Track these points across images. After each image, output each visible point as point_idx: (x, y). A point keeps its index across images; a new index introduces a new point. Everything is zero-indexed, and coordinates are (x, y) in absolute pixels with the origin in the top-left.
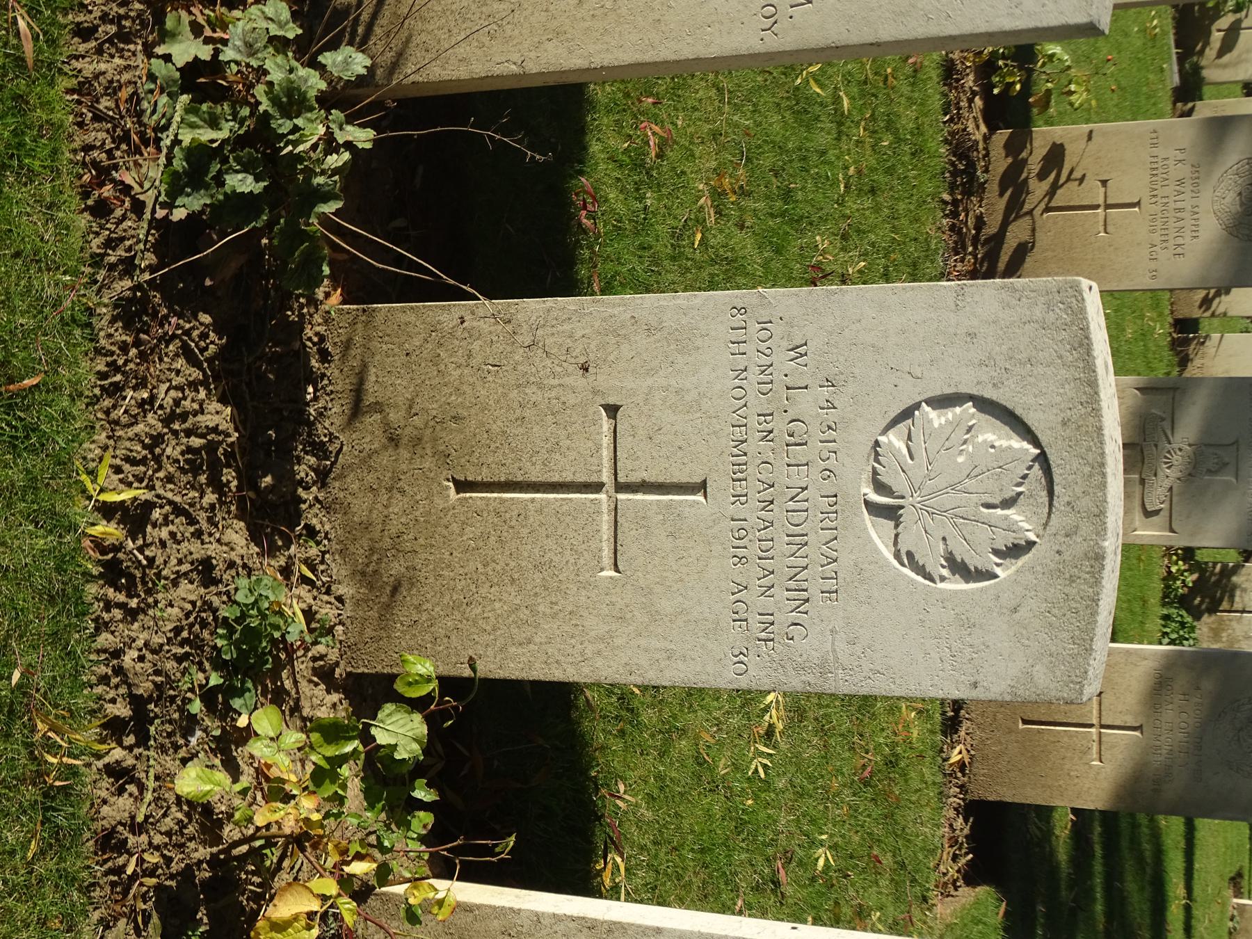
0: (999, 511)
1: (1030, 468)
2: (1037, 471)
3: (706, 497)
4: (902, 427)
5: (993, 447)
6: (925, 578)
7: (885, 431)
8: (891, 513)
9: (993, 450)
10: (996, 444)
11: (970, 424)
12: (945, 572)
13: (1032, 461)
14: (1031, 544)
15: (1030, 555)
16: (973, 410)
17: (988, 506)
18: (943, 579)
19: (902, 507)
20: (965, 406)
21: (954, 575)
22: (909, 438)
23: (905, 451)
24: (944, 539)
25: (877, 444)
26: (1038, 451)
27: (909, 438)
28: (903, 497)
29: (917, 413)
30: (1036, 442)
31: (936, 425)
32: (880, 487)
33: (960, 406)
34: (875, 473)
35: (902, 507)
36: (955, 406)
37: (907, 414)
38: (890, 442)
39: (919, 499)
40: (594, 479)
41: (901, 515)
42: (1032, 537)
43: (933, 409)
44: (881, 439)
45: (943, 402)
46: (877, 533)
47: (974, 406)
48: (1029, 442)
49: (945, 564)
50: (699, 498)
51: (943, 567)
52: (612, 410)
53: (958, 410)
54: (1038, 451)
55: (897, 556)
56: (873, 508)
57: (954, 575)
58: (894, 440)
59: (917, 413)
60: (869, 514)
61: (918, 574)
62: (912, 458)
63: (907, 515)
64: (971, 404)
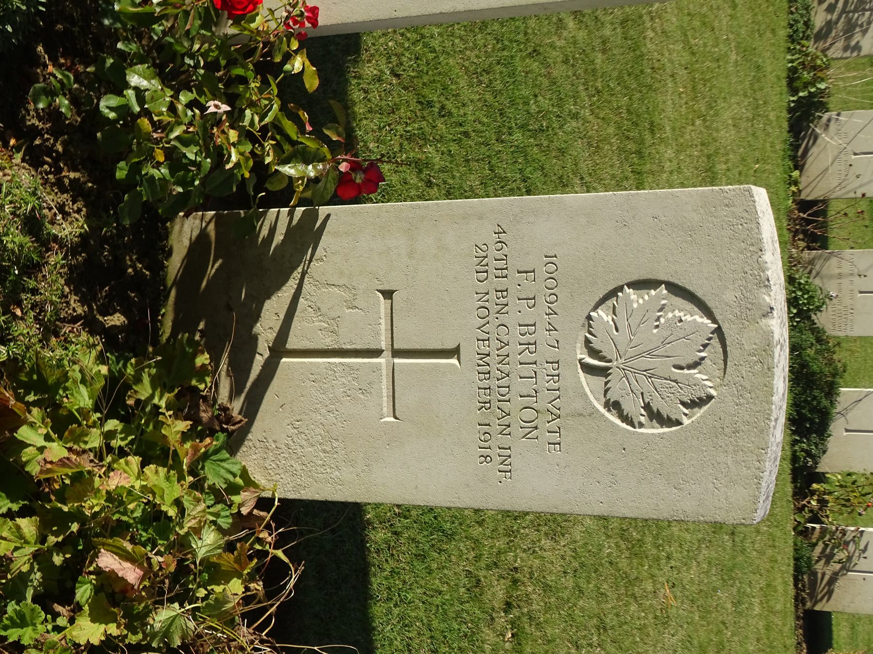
0: (686, 371)
5: (681, 321)
6: (627, 424)
7: (595, 308)
8: (603, 372)
10: (683, 319)
11: (664, 302)
13: (712, 333)
14: (710, 398)
15: (709, 404)
16: (665, 292)
18: (641, 425)
21: (651, 421)
22: (614, 313)
23: (612, 323)
25: (589, 318)
26: (716, 326)
27: (614, 313)
28: (610, 361)
29: (620, 294)
31: (635, 306)
32: (594, 353)
33: (655, 290)
34: (587, 342)
35: (609, 368)
36: (650, 289)
37: (613, 293)
40: (373, 346)
41: (610, 374)
47: (666, 289)
48: (708, 319)
52: (388, 294)
53: (653, 292)
54: (716, 326)
55: (607, 405)
56: (588, 369)
58: (603, 315)
59: (620, 294)
62: (617, 330)
63: (615, 374)
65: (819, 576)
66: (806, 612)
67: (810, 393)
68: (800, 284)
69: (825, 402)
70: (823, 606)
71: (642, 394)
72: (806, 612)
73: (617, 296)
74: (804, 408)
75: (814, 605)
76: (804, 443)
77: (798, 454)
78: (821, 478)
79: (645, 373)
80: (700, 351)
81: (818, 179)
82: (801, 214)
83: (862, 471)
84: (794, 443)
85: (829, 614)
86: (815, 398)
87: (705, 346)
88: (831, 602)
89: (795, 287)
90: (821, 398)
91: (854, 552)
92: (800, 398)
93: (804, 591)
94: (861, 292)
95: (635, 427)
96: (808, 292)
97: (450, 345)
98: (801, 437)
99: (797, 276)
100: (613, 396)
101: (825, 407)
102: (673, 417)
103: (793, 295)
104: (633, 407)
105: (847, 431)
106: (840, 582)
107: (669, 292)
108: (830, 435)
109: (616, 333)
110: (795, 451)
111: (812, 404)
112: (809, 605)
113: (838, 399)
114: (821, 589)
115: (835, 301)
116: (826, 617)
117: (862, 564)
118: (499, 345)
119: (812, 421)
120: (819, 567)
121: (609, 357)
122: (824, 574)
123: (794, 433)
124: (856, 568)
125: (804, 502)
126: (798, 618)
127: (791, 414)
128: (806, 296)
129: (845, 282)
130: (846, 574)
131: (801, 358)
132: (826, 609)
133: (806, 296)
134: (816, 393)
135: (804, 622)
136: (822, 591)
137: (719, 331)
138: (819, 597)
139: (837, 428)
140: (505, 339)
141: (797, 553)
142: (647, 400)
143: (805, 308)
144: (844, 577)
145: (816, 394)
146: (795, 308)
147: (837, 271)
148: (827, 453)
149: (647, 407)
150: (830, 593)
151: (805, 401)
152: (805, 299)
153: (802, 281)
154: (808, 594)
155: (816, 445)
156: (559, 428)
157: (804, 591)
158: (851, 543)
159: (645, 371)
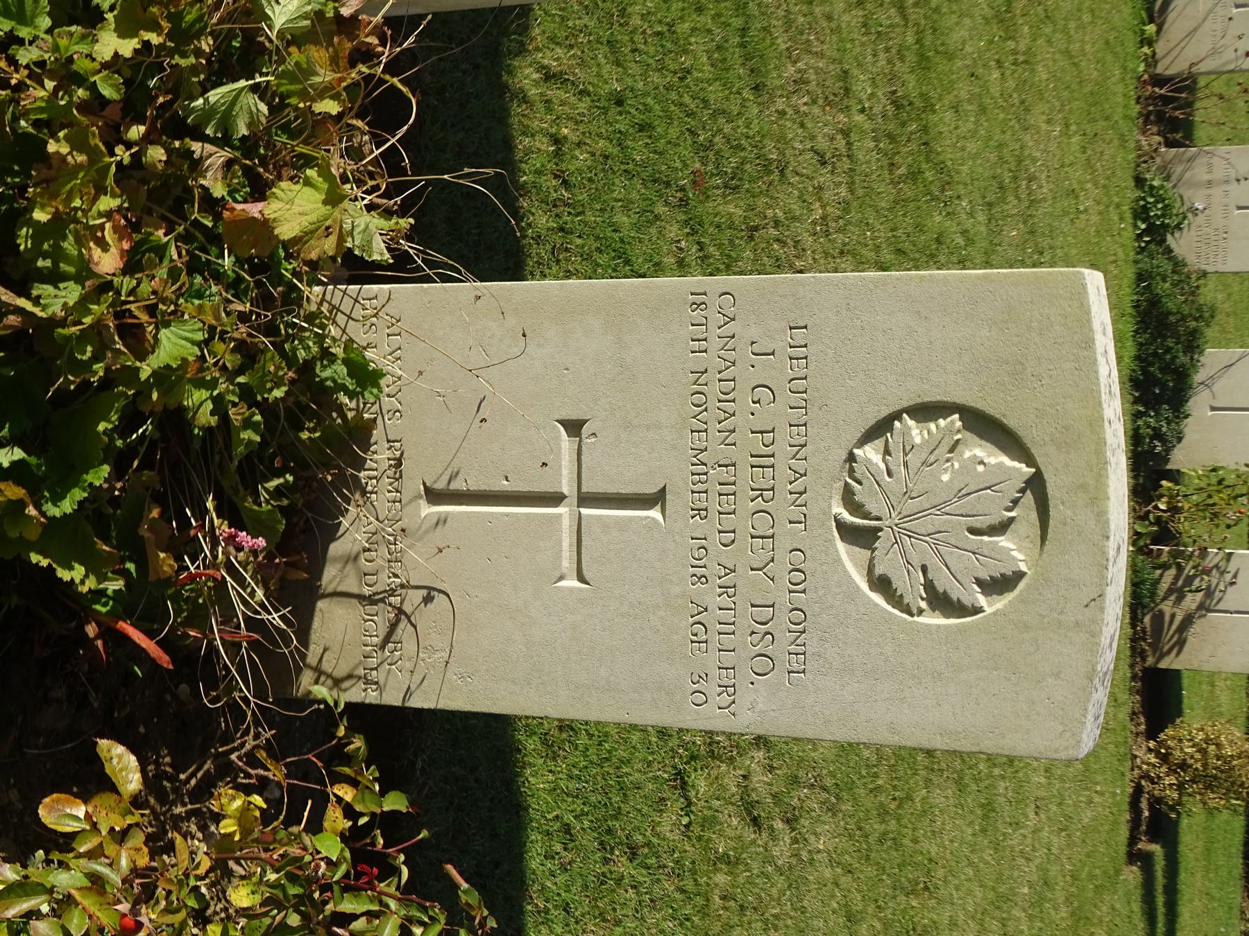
0: (986, 538)
1: (1023, 491)
2: (1029, 496)
3: (663, 512)
4: (879, 443)
5: (982, 462)
6: (902, 611)
9: (980, 468)
10: (985, 461)
11: (959, 436)
12: (923, 605)
14: (1021, 575)
16: (959, 424)
17: (973, 531)
18: (921, 612)
19: (881, 530)
20: (949, 419)
23: (883, 466)
24: (924, 569)
25: (851, 458)
27: (887, 452)
29: (897, 423)
30: (1029, 460)
38: (869, 460)
39: (897, 521)
42: (1023, 567)
43: (918, 421)
44: (856, 451)
45: (925, 411)
46: (849, 558)
47: (961, 419)
49: (924, 596)
50: (655, 513)
51: (923, 599)
53: (942, 422)
56: (848, 532)
57: (934, 611)
58: (871, 453)
59: (897, 423)
60: (842, 539)
61: (894, 607)
62: (890, 474)
64: (956, 416)
65: (1167, 618)
66: (1146, 671)
67: (1162, 343)
68: (1152, 187)
69: (1183, 359)
70: (1172, 662)
71: (924, 569)
72: (1146, 671)
73: (891, 429)
74: (1153, 364)
75: (1158, 661)
76: (1151, 417)
77: (1141, 431)
78: (1175, 476)
79: (927, 538)
80: (1009, 509)
81: (1182, 44)
82: (1157, 90)
83: (1233, 467)
84: (1137, 415)
85: (1177, 673)
86: (1168, 350)
87: (1015, 502)
88: (1182, 656)
89: (1144, 192)
90: (1178, 351)
91: (1218, 584)
92: (1147, 349)
93: (1145, 640)
94: (1239, 208)
95: (912, 615)
96: (1163, 201)
97: (652, 489)
98: (1148, 409)
99: (1148, 176)
100: (879, 570)
101: (1183, 365)
102: (967, 601)
103: (1142, 203)
104: (911, 587)
105: (1213, 409)
106: (1197, 627)
107: (967, 427)
108: (1187, 416)
109: (887, 479)
110: (1139, 427)
111: (1164, 359)
112: (1150, 661)
113: (1201, 358)
114: (1168, 637)
115: (1201, 218)
116: (1175, 675)
117: (1231, 599)
118: (722, 320)
119: (1163, 386)
120: (1167, 607)
121: (875, 513)
122: (1173, 616)
123: (1136, 401)
124: (1221, 606)
125: (1150, 508)
126: (1134, 677)
127: (1134, 371)
128: (1160, 206)
129: (1217, 192)
130: (1205, 615)
131: (1151, 292)
132: (1175, 666)
133: (1160, 206)
134: (1170, 342)
135: (1143, 684)
136: (1170, 640)
137: (1036, 484)
138: (1166, 648)
139: (1198, 405)
140: (731, 311)
141: (1136, 577)
142: (930, 576)
143: (1158, 223)
144: (1203, 620)
145: (1171, 345)
146: (1144, 221)
147: (1207, 177)
148: (1184, 441)
149: (929, 586)
150: (1181, 643)
151: (1155, 354)
152: (1158, 209)
153: (1155, 183)
154: (1150, 645)
155: (1169, 423)
156: (805, 516)
157: (1145, 640)
158: (1214, 571)
159: (928, 535)
